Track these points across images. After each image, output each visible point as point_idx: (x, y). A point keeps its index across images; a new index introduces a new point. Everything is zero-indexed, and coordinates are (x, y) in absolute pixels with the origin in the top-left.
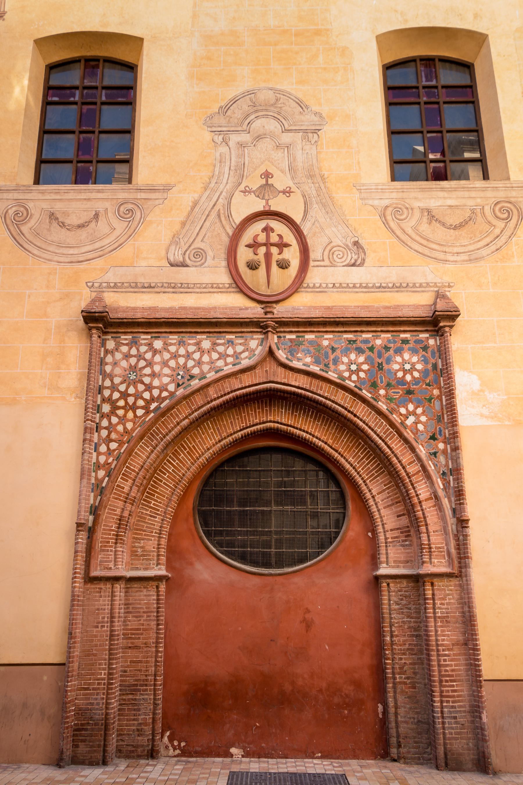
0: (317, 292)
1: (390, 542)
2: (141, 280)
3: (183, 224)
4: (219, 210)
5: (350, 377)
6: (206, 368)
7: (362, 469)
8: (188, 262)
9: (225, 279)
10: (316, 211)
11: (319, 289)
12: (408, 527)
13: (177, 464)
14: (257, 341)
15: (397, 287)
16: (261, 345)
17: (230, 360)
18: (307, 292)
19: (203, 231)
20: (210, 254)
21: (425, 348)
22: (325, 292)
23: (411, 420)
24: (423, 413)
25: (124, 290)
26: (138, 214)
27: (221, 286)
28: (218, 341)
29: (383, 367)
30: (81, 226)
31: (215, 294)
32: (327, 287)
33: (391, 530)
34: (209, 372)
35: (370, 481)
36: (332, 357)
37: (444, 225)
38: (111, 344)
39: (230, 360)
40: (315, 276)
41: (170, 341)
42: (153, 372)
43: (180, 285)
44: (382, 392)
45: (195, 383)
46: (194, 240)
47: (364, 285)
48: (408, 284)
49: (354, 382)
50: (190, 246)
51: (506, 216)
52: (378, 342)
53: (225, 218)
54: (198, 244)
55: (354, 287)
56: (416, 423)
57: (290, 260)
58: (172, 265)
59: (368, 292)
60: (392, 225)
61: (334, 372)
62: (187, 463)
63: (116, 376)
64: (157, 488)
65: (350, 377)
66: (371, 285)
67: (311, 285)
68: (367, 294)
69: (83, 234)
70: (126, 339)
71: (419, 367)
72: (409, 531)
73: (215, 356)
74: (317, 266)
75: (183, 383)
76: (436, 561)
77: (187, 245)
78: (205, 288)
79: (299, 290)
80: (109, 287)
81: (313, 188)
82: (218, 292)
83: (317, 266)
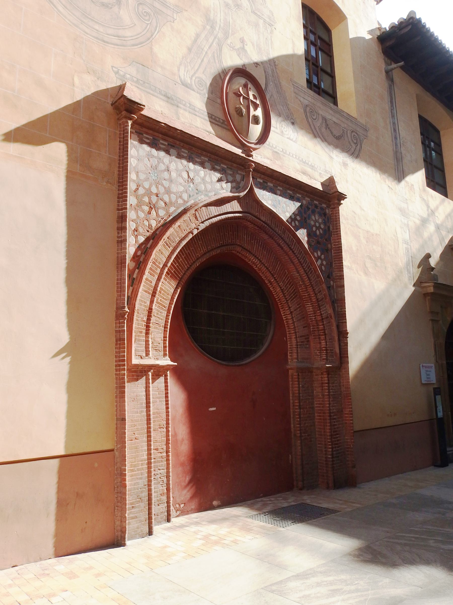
1: (300, 345)
4: (214, 52)
7: (287, 291)
10: (271, 86)
12: (308, 335)
16: (243, 181)
21: (325, 214)
23: (319, 262)
25: (143, 88)
28: (216, 166)
35: (291, 301)
37: (332, 133)
41: (182, 153)
51: (355, 141)
53: (218, 61)
58: (183, 84)
60: (310, 120)
62: (185, 267)
67: (271, 145)
70: (148, 139)
71: (322, 226)
72: (308, 338)
75: (193, 195)
81: (270, 69)
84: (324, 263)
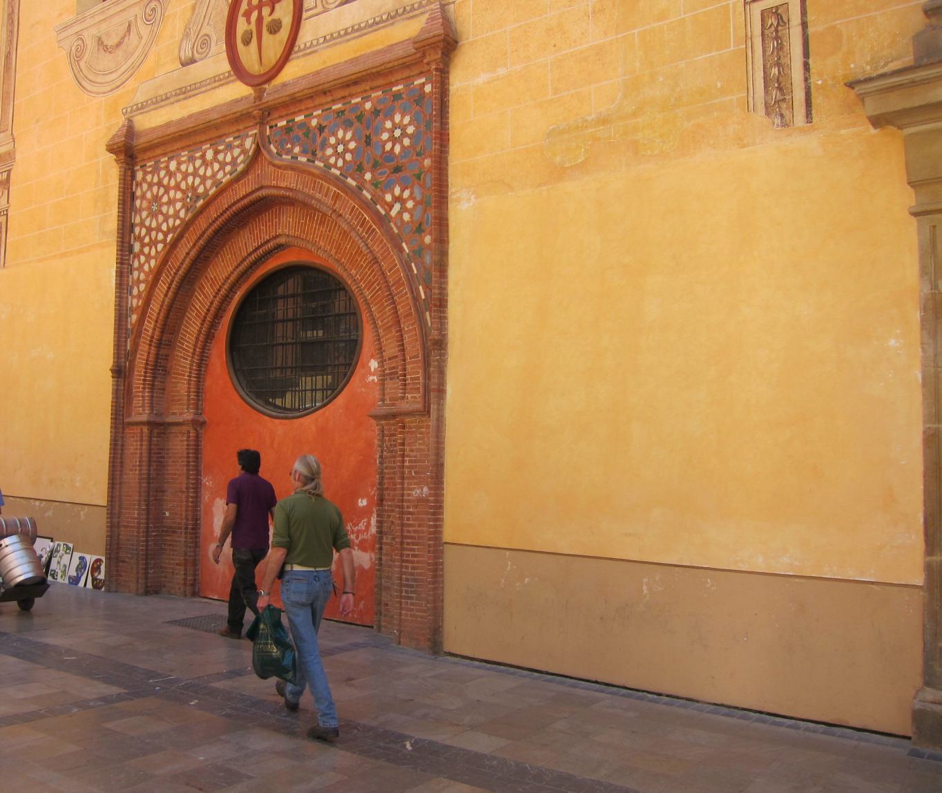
0: (310, 54)
2: (161, 92)
3: (194, 8)
5: (336, 162)
6: (209, 183)
8: (197, 56)
9: (225, 66)
11: (311, 50)
13: (203, 299)
14: (251, 138)
15: (392, 18)
17: (228, 168)
18: (298, 57)
19: (209, 12)
20: (214, 38)
22: (315, 52)
24: (411, 197)
26: (159, 10)
27: (222, 77)
29: (370, 140)
30: (119, 45)
31: (217, 89)
32: (318, 44)
33: (390, 359)
34: (211, 188)
36: (319, 140)
38: (139, 175)
39: (228, 168)
40: (307, 34)
42: (169, 198)
43: (189, 88)
44: (368, 176)
45: (201, 202)
46: (202, 25)
47: (356, 27)
48: (405, 8)
49: (339, 169)
50: (198, 36)
52: (368, 106)
54: (204, 31)
55: (346, 34)
56: (400, 213)
57: (282, 19)
58: (184, 65)
59: (361, 36)
61: (320, 161)
63: (143, 210)
64: (188, 328)
65: (336, 162)
66: (362, 25)
67: (302, 46)
68: (359, 40)
69: (120, 53)
73: (216, 166)
74: (310, 17)
76: (409, 396)
77: (196, 34)
78: (209, 84)
79: (291, 57)
80: (138, 109)
82: (222, 85)
83: (310, 17)
84: (410, 204)
